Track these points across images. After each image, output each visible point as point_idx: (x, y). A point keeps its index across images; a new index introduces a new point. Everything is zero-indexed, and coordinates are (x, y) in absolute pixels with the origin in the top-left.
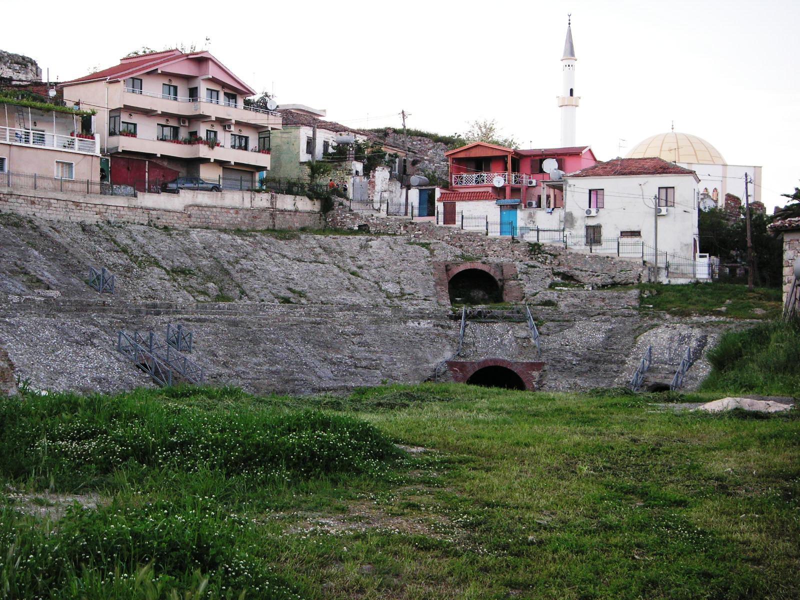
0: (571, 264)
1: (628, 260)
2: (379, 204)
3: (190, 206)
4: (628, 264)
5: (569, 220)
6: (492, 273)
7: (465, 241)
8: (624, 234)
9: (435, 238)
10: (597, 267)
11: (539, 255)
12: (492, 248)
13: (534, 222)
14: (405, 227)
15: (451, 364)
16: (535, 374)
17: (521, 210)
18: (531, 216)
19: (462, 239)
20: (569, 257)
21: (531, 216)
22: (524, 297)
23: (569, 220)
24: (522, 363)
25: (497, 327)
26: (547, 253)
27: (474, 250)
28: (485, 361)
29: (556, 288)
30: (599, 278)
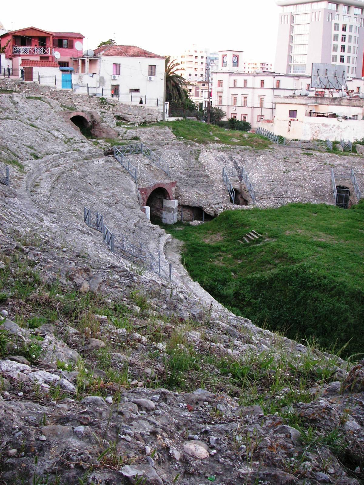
0: (123, 111)
1: (151, 108)
4: (152, 110)
5: (102, 81)
6: (86, 118)
7: (60, 96)
8: (131, 90)
9: (40, 93)
10: (136, 112)
11: (106, 105)
12: (77, 100)
13: (82, 82)
14: (19, 85)
16: (173, 189)
17: (74, 74)
18: (80, 78)
19: (58, 95)
20: (121, 106)
21: (80, 78)
22: (119, 135)
23: (102, 81)
26: (109, 104)
27: (66, 101)
29: (122, 126)
30: (138, 119)
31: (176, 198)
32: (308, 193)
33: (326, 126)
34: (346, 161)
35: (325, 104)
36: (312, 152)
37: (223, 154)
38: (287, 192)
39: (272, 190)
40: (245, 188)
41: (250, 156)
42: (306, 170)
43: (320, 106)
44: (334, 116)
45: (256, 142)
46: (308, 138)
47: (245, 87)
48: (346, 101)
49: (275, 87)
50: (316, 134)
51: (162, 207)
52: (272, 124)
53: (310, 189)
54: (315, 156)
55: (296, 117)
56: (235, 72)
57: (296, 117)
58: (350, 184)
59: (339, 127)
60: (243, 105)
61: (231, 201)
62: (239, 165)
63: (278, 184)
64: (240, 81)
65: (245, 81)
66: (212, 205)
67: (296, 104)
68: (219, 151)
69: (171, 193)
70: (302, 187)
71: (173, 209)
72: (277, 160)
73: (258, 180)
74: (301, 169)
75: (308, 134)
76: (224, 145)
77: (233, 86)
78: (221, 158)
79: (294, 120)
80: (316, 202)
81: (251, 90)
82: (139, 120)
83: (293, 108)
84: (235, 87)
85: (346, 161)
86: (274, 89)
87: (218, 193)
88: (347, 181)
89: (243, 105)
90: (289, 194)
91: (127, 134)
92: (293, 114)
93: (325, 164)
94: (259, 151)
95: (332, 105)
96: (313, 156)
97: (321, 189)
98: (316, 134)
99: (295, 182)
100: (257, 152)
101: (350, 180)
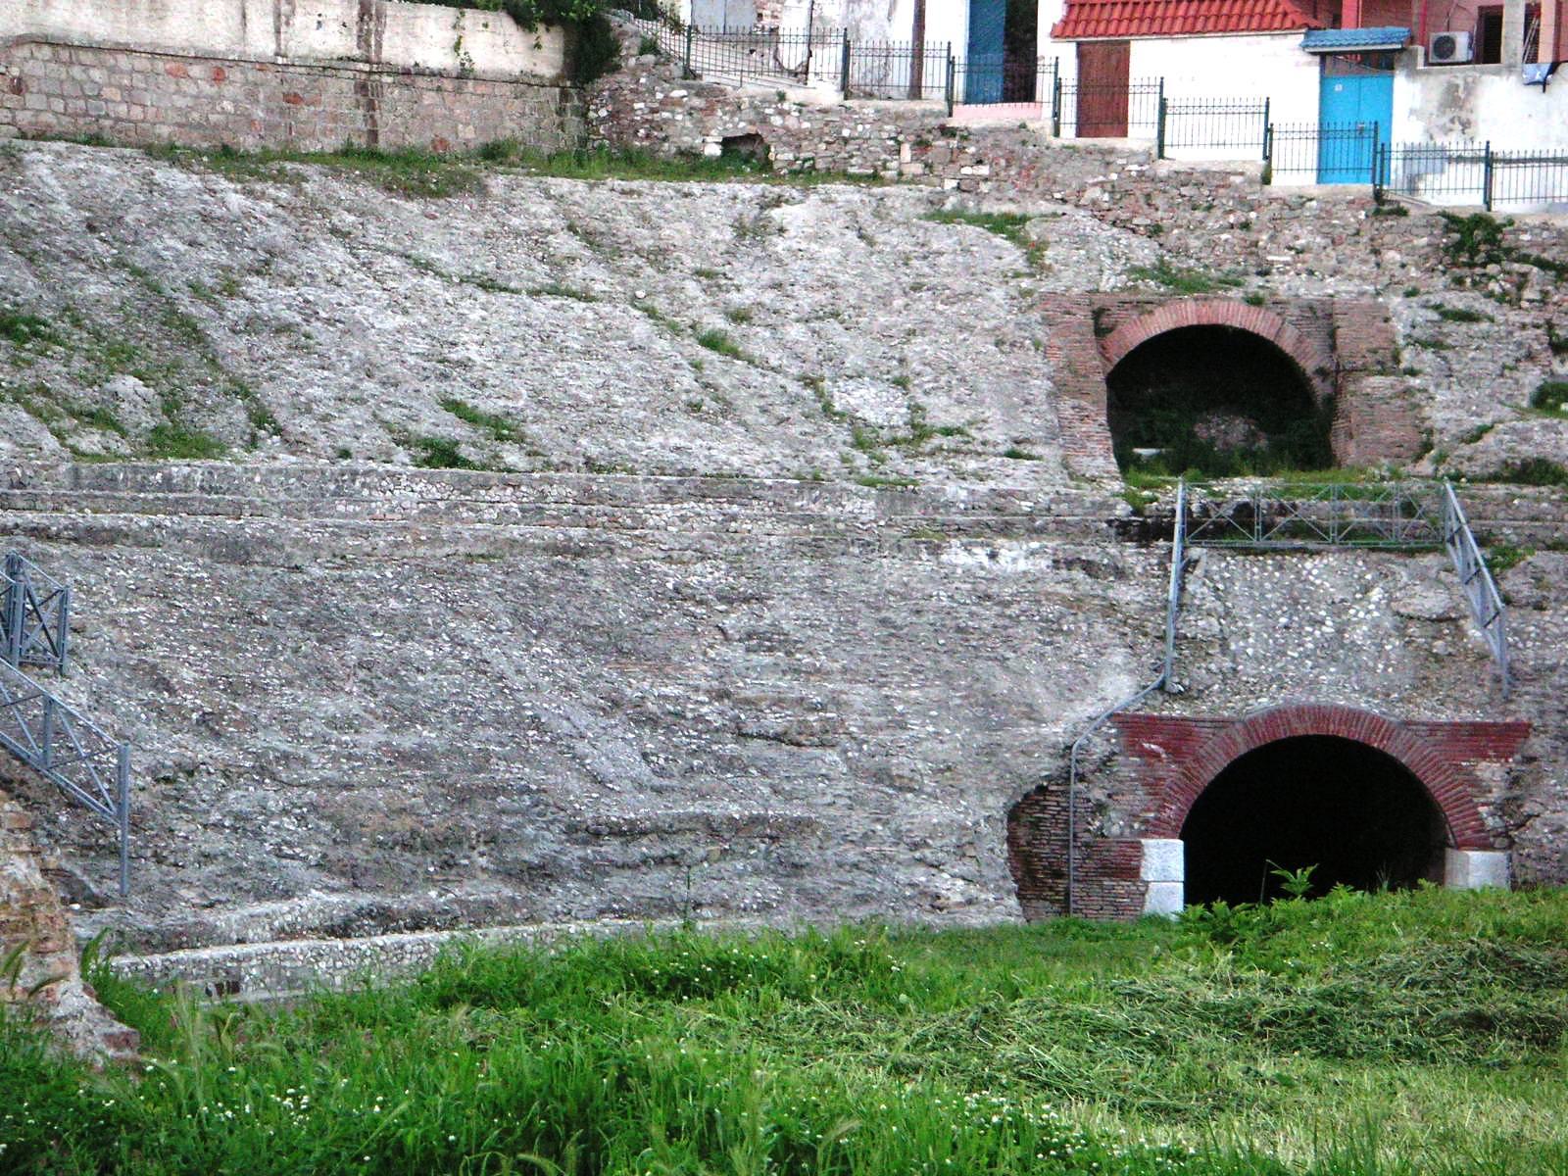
2: (803, 49)
3: (20, 41)
6: (1287, 344)
7: (1171, 207)
9: (1046, 195)
11: (1492, 269)
12: (1287, 235)
13: (1466, 125)
14: (921, 145)
15: (1132, 727)
16: (1491, 771)
17: (1413, 73)
18: (1455, 102)
19: (1159, 200)
22: (1427, 447)
24: (1434, 728)
25: (1323, 571)
26: (1524, 259)
27: (1212, 245)
28: (1273, 717)
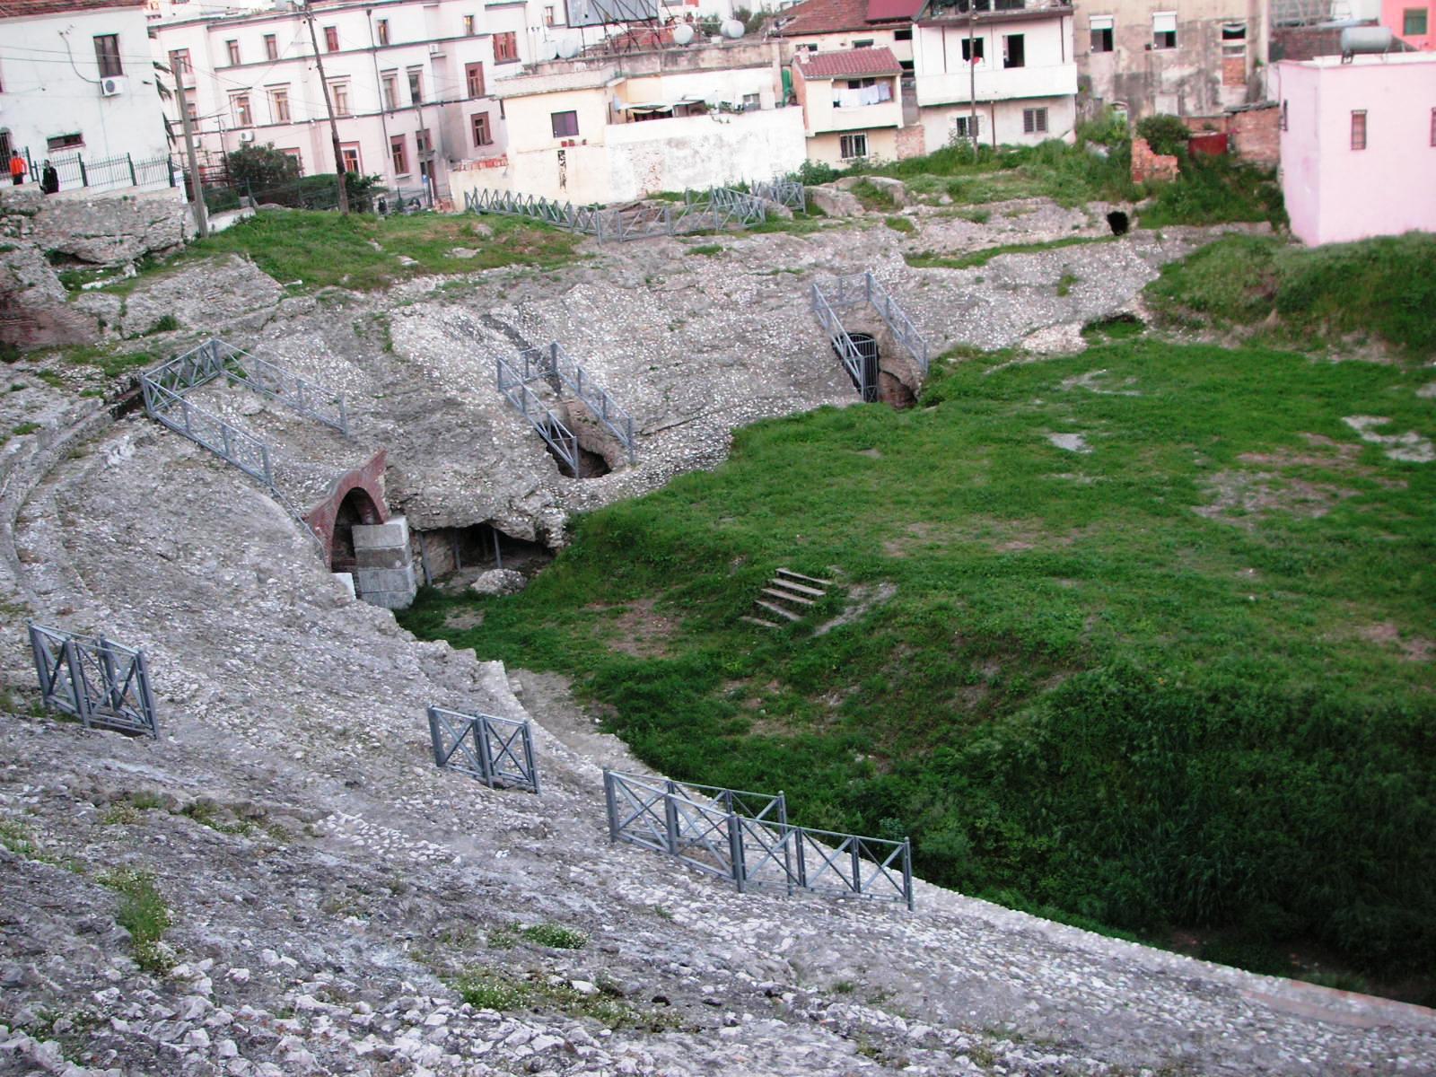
0: (65, 227)
1: (156, 197)
4: (161, 204)
10: (111, 224)
20: (57, 212)
22: (103, 324)
26: (13, 212)
29: (86, 286)
30: (126, 246)
31: (398, 511)
32: (769, 379)
33: (679, 144)
34: (829, 250)
35: (648, 76)
36: (716, 240)
37: (458, 312)
38: (709, 394)
39: (667, 398)
40: (581, 412)
41: (543, 298)
42: (734, 306)
43: (631, 82)
44: (698, 108)
45: (530, 244)
46: (630, 195)
47: (273, 59)
48: (715, 53)
49: (378, 44)
50: (652, 176)
51: (353, 555)
52: (502, 169)
53: (771, 367)
54: (734, 255)
55: (577, 133)
56: (223, 16)
57: (577, 133)
58: (873, 320)
59: (721, 143)
60: (276, 120)
61: (565, 470)
62: (526, 336)
63: (672, 375)
64: (251, 42)
65: (270, 39)
66: (517, 503)
67: (571, 90)
68: (443, 305)
69: (380, 499)
70: (744, 365)
71: (397, 553)
72: (630, 292)
73: (612, 376)
74: (713, 304)
75: (629, 182)
76: (440, 280)
77: (226, 63)
78: (461, 327)
79: (572, 144)
80: (805, 407)
81: (296, 65)
82: (126, 250)
83: (562, 104)
84: (235, 64)
85: (829, 250)
86: (374, 50)
87: (517, 452)
88: (861, 314)
89: (276, 120)
90: (718, 398)
91: (131, 313)
92: (564, 124)
93: (776, 272)
94: (561, 272)
95: (672, 73)
96: (725, 255)
97: (804, 358)
98: (652, 176)
99: (716, 355)
100: (557, 279)
101: (869, 311)
